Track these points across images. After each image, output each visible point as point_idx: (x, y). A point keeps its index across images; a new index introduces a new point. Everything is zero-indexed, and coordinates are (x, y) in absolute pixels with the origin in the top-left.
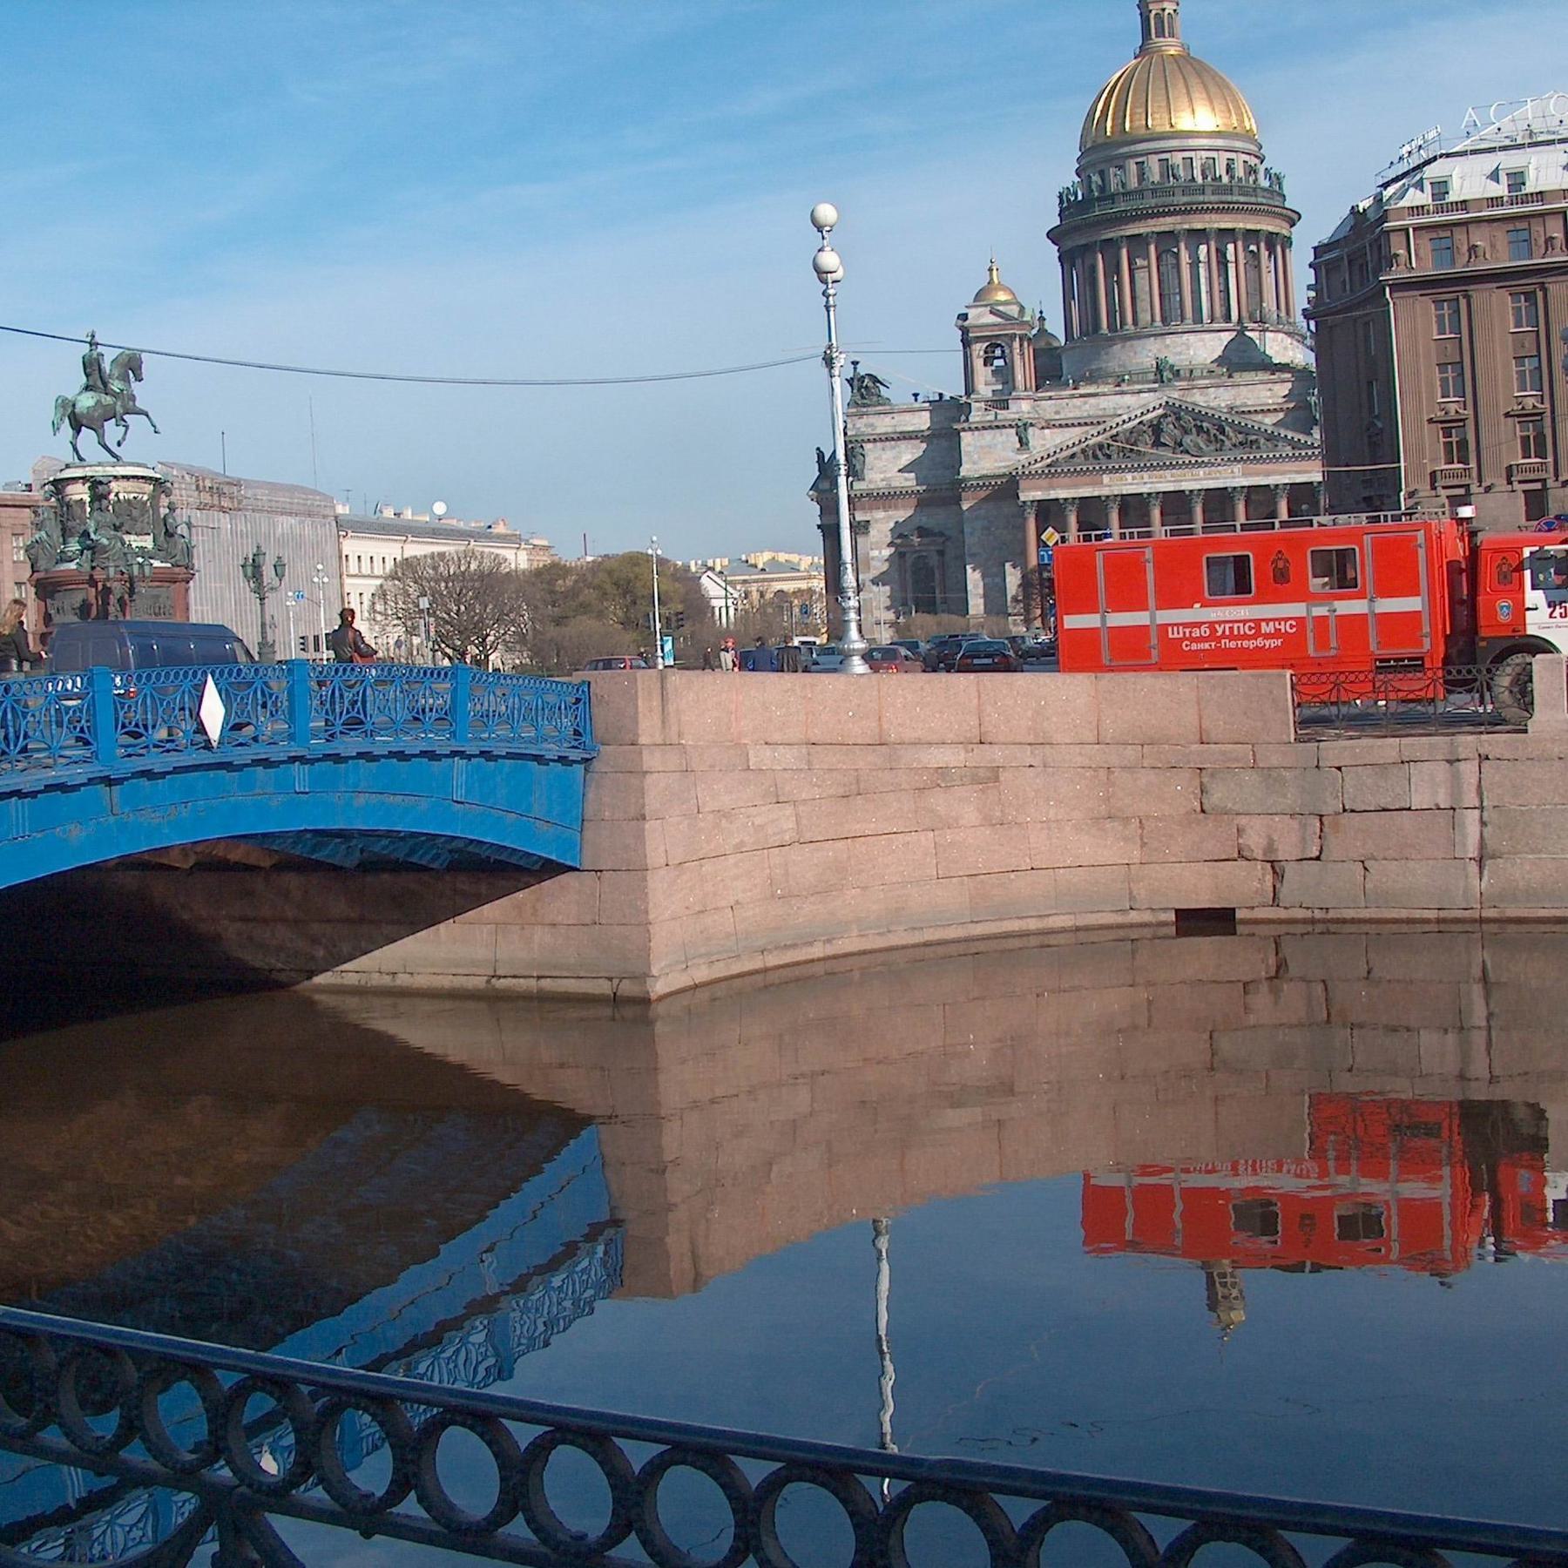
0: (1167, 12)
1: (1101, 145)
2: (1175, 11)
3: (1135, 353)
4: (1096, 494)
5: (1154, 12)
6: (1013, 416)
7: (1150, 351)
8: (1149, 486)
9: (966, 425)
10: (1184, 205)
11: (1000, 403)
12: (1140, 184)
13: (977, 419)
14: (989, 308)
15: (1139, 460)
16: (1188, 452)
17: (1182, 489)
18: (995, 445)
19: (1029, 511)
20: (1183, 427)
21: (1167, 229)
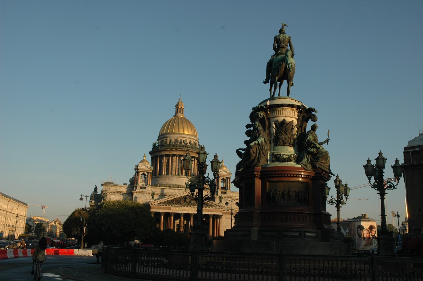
0: (182, 108)
1: (163, 134)
2: (184, 108)
3: (171, 181)
4: (169, 212)
5: (179, 108)
6: (147, 191)
7: (174, 181)
8: (182, 211)
9: (135, 191)
10: (186, 149)
11: (143, 188)
12: (170, 144)
13: (138, 191)
14: (144, 165)
15: (181, 205)
16: (192, 204)
17: (189, 213)
18: (142, 197)
19: (162, 214)
20: (191, 199)
21: (181, 154)
